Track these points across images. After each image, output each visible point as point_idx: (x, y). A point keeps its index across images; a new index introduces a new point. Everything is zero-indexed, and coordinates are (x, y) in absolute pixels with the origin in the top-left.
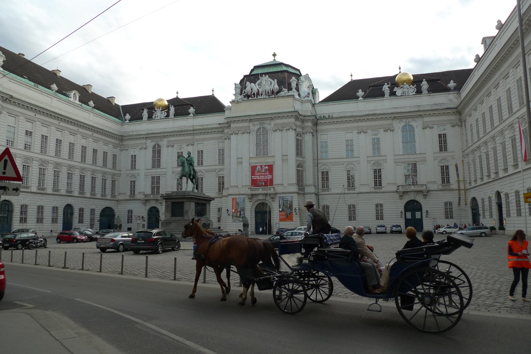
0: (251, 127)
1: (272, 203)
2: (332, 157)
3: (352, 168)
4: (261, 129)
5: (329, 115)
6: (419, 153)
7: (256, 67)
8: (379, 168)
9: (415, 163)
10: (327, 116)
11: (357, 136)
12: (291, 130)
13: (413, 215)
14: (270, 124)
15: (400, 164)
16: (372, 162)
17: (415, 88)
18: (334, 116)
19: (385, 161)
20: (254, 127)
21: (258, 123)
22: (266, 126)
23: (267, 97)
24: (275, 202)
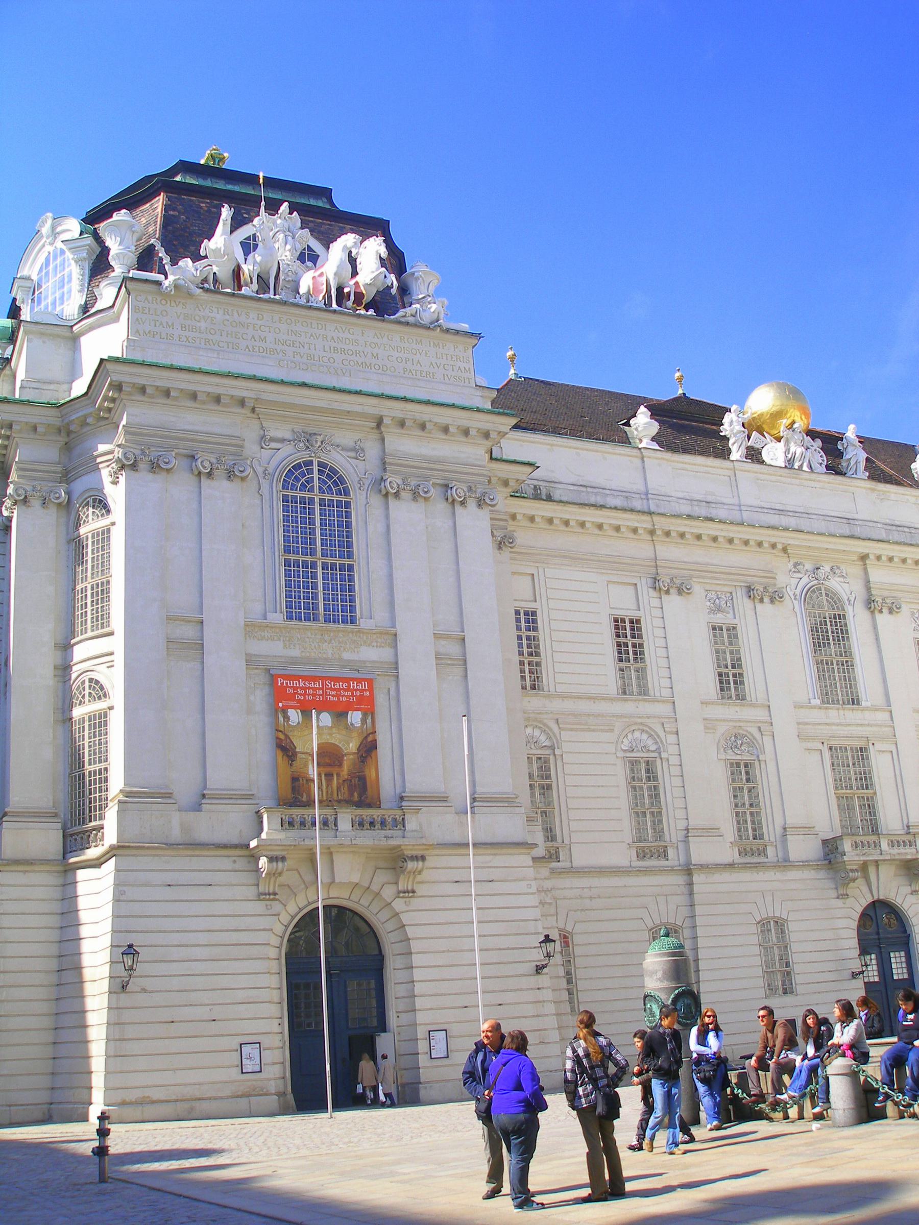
0: (251, 448)
1: (398, 905)
2: (560, 688)
3: (649, 751)
4: (310, 471)
5: (535, 487)
6: (869, 704)
7: (185, 167)
8: (746, 757)
9: (862, 744)
10: (530, 491)
11: (655, 602)
12: (472, 504)
13: (885, 968)
14: (357, 451)
15: (820, 746)
16: (722, 729)
17: (822, 453)
18: (557, 495)
19: (766, 727)
20: (266, 454)
21: (288, 435)
22: (338, 460)
23: (334, 305)
24: (416, 903)
